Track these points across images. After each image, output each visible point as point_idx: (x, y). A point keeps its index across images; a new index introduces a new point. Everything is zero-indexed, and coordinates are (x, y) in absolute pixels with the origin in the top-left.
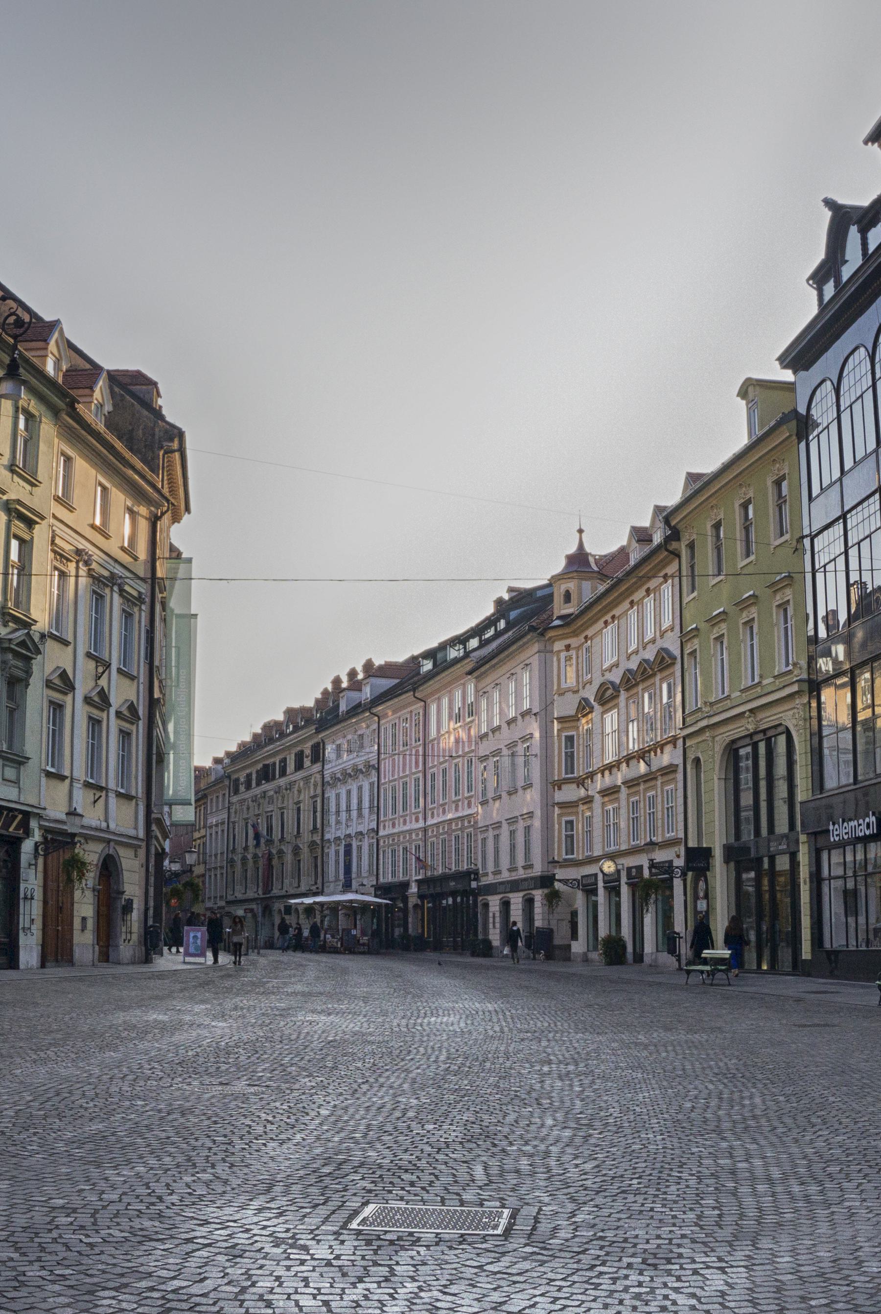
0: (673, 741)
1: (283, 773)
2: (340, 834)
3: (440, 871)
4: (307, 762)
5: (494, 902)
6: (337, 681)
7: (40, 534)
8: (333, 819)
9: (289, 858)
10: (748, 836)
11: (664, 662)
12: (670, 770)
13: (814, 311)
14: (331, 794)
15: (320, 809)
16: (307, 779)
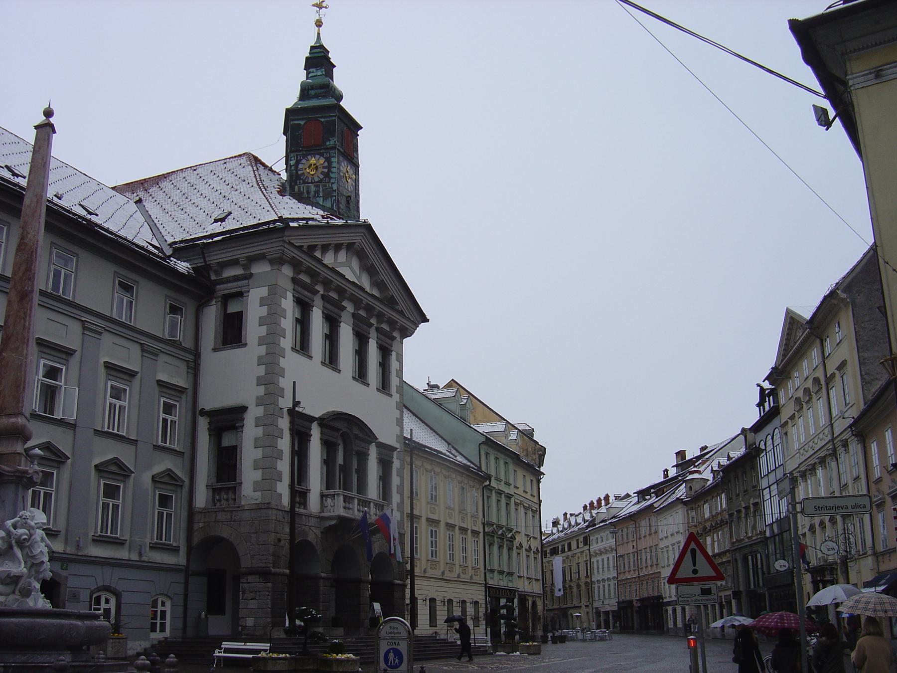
0: (728, 551)
1: (570, 549)
2: (600, 578)
3: (645, 595)
4: (581, 545)
5: (670, 609)
6: (592, 503)
7: (512, 500)
8: (596, 571)
9: (575, 589)
10: (752, 586)
11: (723, 523)
12: (729, 562)
13: (757, 418)
14: (594, 560)
15: (589, 565)
16: (582, 552)
